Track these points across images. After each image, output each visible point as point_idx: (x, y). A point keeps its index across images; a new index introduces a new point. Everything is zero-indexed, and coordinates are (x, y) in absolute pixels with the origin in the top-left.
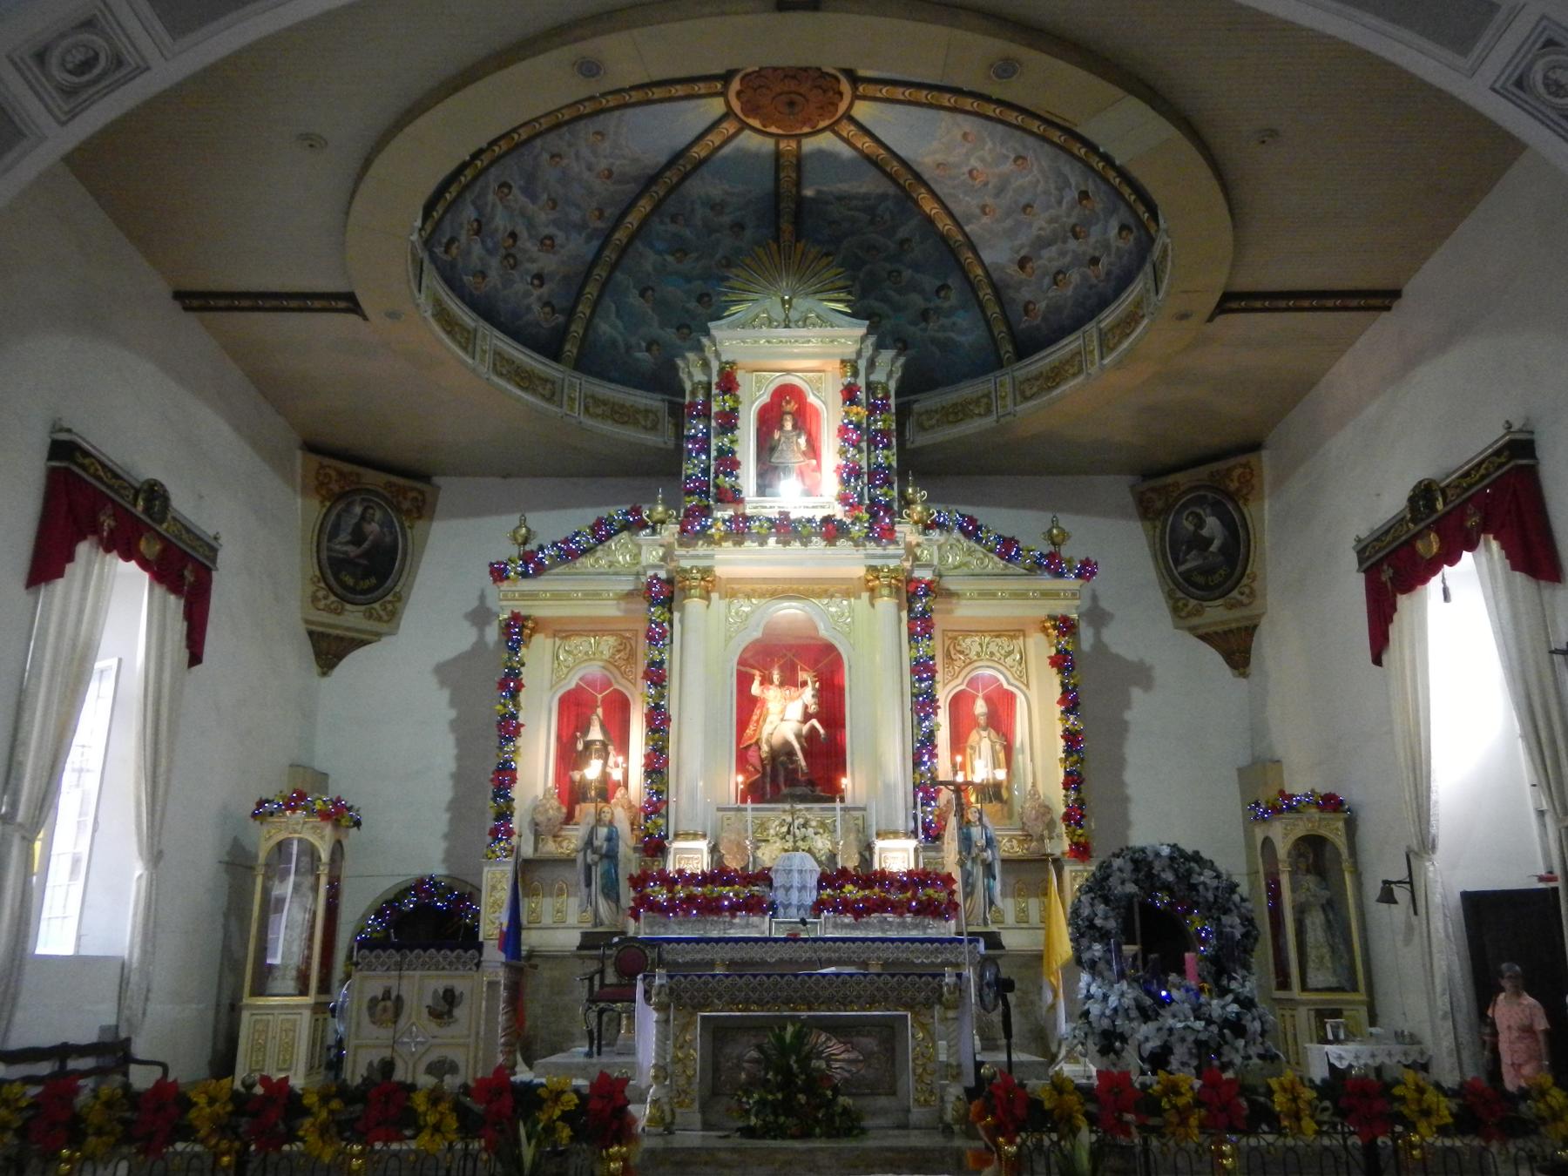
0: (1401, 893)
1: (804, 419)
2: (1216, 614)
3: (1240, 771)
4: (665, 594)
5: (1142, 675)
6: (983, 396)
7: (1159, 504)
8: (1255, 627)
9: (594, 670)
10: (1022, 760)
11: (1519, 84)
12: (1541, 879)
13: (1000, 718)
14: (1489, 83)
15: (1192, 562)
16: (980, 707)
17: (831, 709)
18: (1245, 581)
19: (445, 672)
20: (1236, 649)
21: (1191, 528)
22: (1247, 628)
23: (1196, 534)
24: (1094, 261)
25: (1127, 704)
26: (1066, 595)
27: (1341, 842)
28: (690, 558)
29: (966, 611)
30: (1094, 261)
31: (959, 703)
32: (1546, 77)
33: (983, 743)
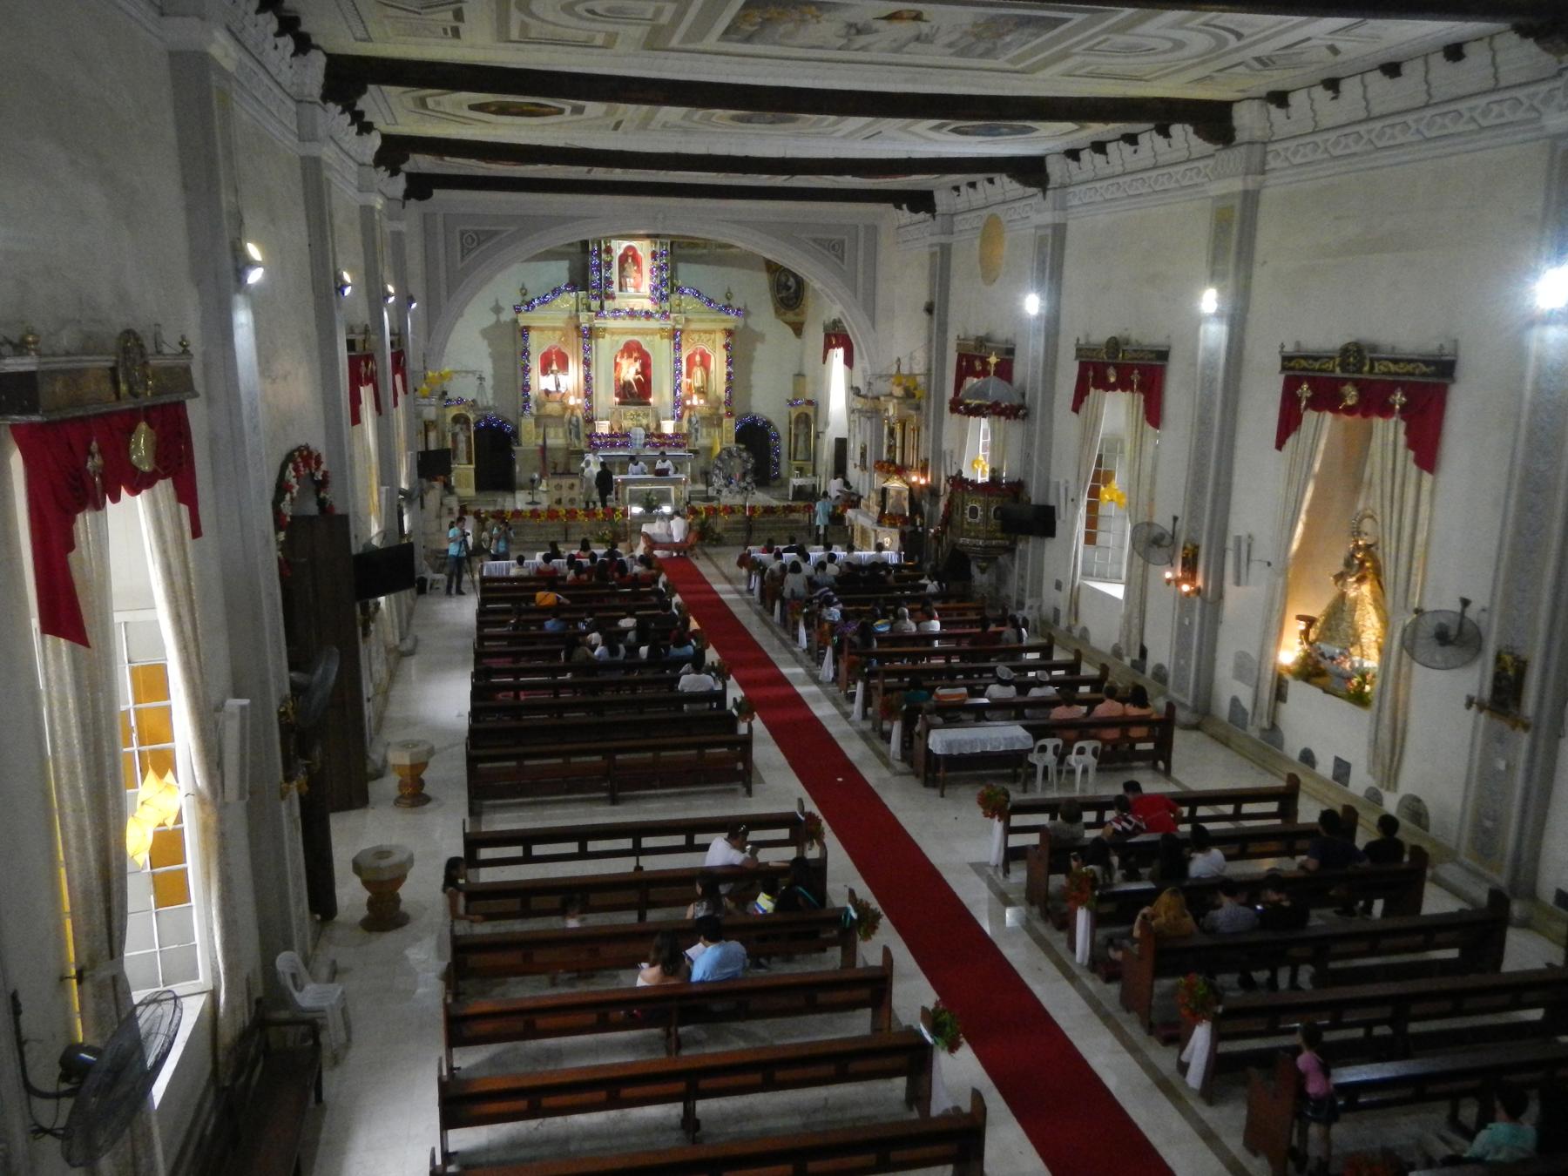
1: (636, 260)
2: (790, 316)
4: (590, 334)
5: (760, 337)
9: (554, 343)
10: (712, 376)
13: (705, 362)
15: (784, 294)
16: (698, 358)
17: (645, 369)
19: (485, 333)
20: (798, 329)
25: (754, 349)
26: (731, 321)
27: (812, 414)
28: (598, 323)
29: (693, 326)
31: (690, 359)
33: (698, 372)
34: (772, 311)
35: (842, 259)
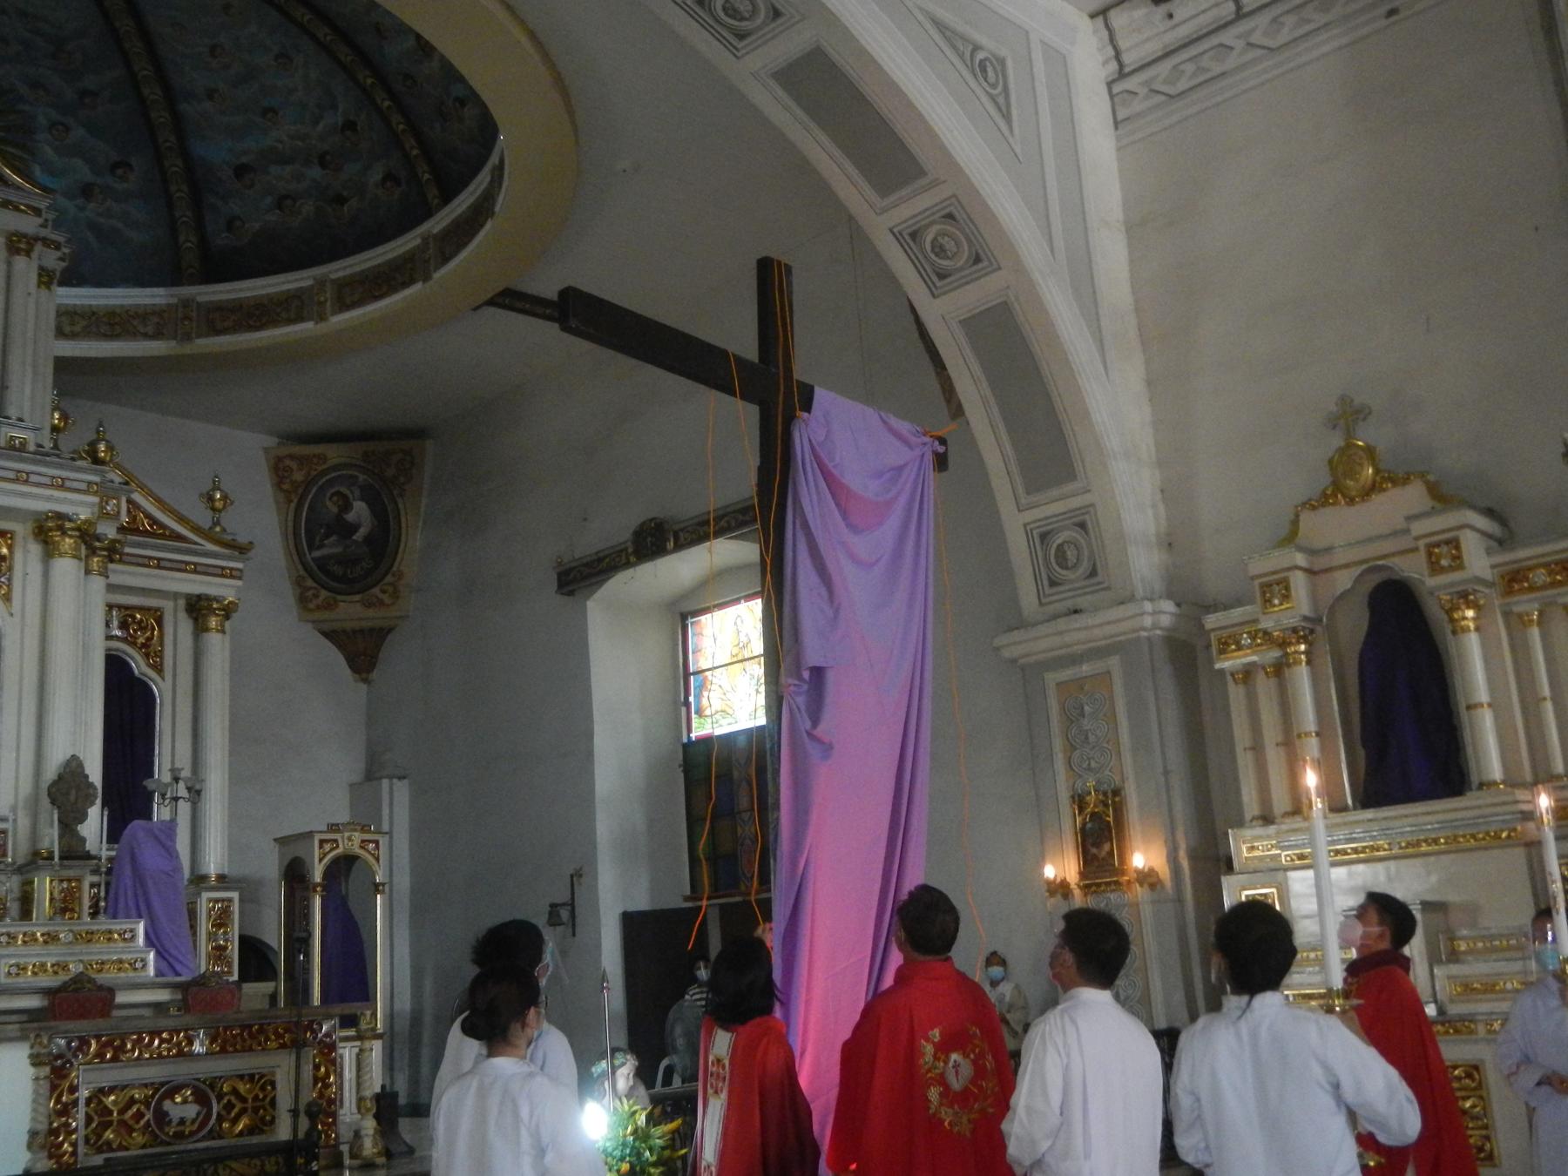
0: (564, 914)
2: (351, 612)
3: (351, 785)
6: (154, 313)
7: (298, 476)
8: (390, 630)
11: (913, 235)
12: (686, 899)
14: (891, 224)
15: (332, 548)
18: (389, 579)
21: (335, 510)
22: (381, 629)
23: (339, 518)
24: (340, 200)
30: (340, 200)
32: (935, 240)
34: (291, 600)
35: (1007, 117)
